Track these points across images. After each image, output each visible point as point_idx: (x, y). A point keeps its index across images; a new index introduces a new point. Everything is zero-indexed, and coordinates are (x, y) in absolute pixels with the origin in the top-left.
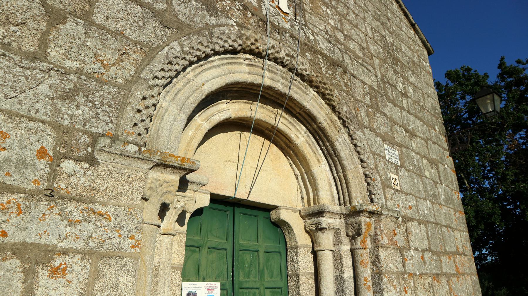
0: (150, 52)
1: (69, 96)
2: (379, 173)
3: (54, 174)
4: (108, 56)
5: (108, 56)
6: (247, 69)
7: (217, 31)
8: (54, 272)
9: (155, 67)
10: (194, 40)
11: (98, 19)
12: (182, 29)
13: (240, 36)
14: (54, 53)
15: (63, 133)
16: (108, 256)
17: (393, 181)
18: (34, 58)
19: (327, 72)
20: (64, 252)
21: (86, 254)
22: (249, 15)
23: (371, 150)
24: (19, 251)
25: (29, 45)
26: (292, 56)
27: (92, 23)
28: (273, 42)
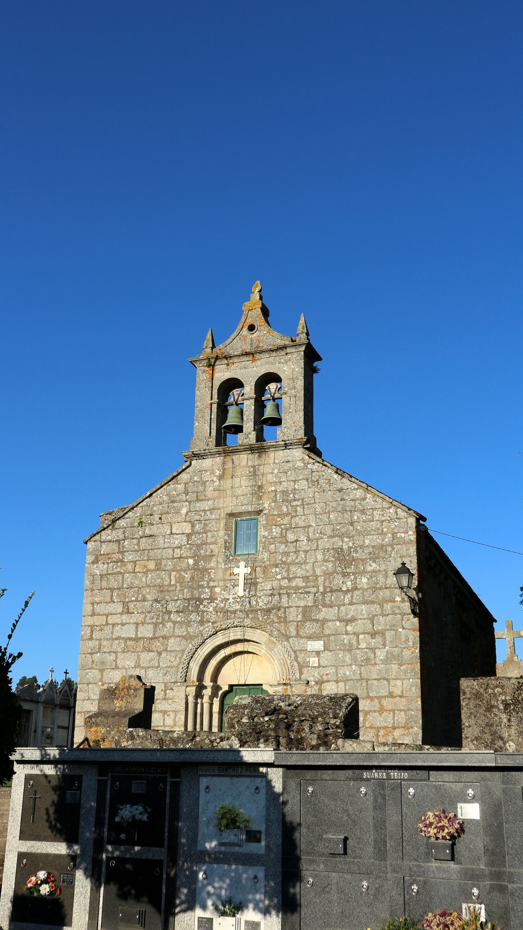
0: (183, 651)
1: (165, 674)
2: (297, 660)
3: (165, 694)
4: (172, 659)
5: (172, 659)
6: (222, 637)
7: (204, 632)
8: (168, 715)
9: (185, 657)
10: (196, 640)
11: (169, 649)
12: (192, 638)
13: (214, 627)
14: (161, 664)
15: (165, 684)
16: (178, 711)
17: (311, 663)
18: (157, 667)
19: (262, 619)
20: (169, 711)
21: (173, 711)
22: (219, 613)
23: (292, 649)
24: (161, 711)
25: (156, 665)
26: (240, 622)
27: (168, 651)
28: (229, 621)
